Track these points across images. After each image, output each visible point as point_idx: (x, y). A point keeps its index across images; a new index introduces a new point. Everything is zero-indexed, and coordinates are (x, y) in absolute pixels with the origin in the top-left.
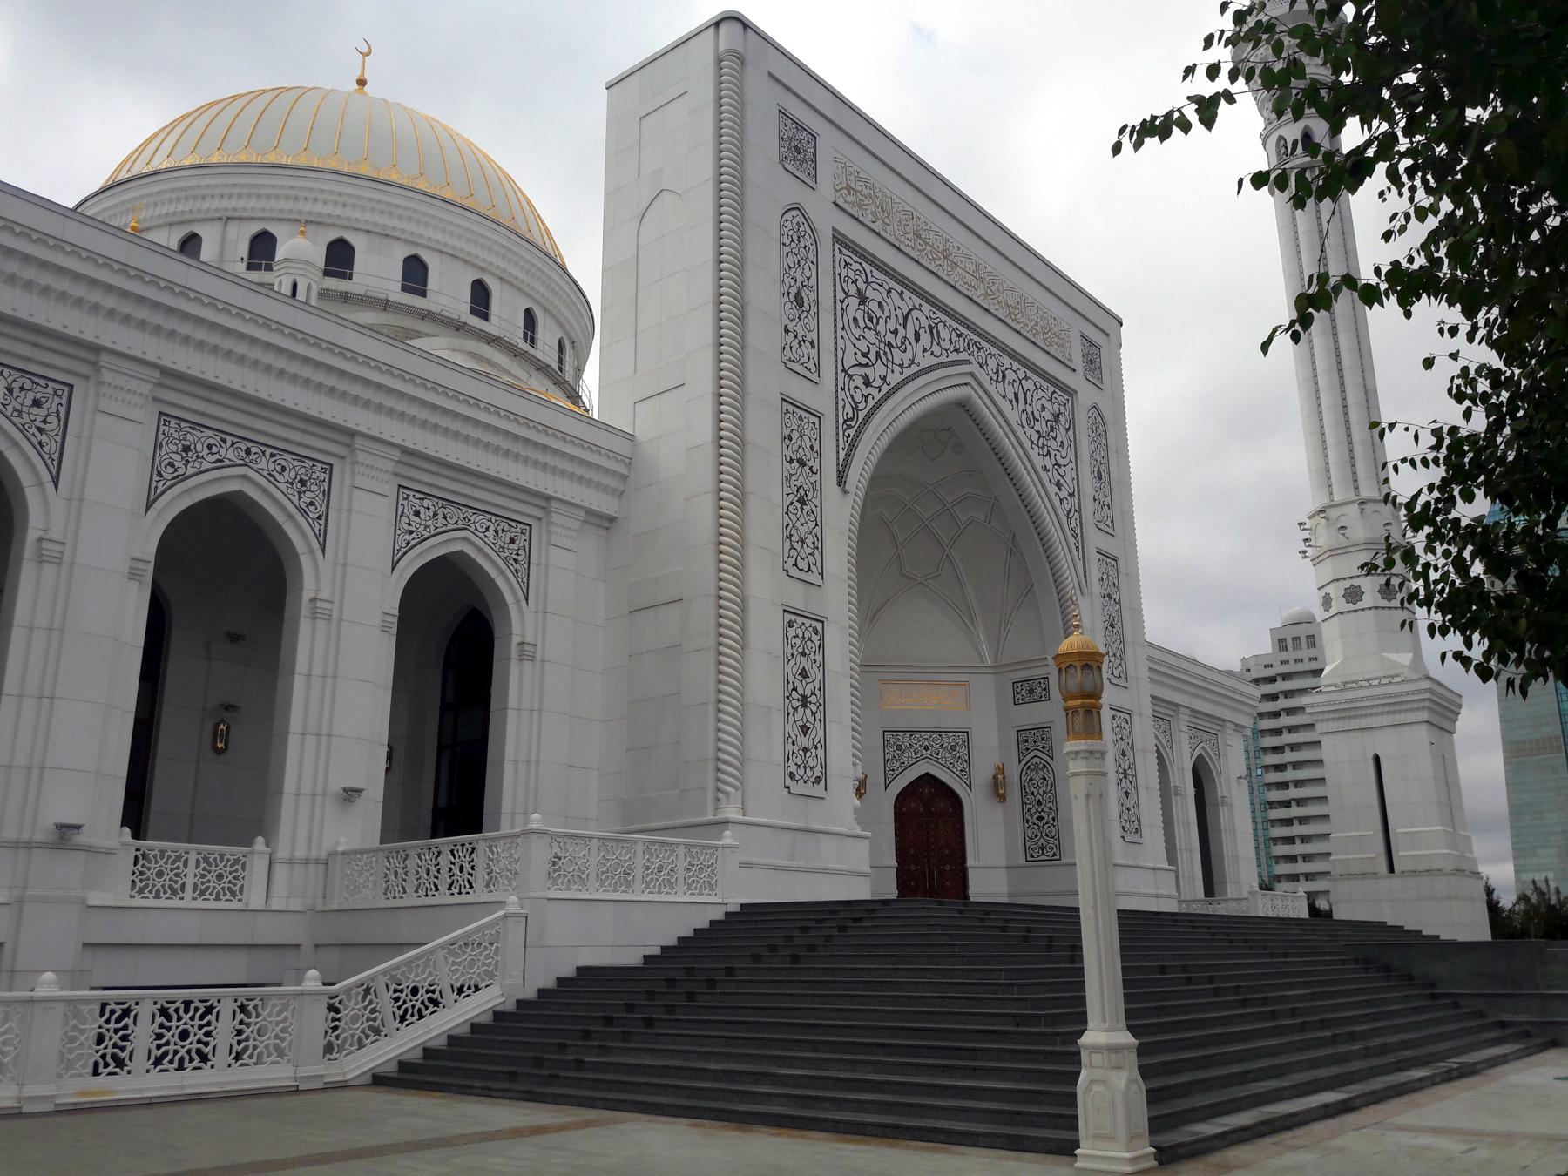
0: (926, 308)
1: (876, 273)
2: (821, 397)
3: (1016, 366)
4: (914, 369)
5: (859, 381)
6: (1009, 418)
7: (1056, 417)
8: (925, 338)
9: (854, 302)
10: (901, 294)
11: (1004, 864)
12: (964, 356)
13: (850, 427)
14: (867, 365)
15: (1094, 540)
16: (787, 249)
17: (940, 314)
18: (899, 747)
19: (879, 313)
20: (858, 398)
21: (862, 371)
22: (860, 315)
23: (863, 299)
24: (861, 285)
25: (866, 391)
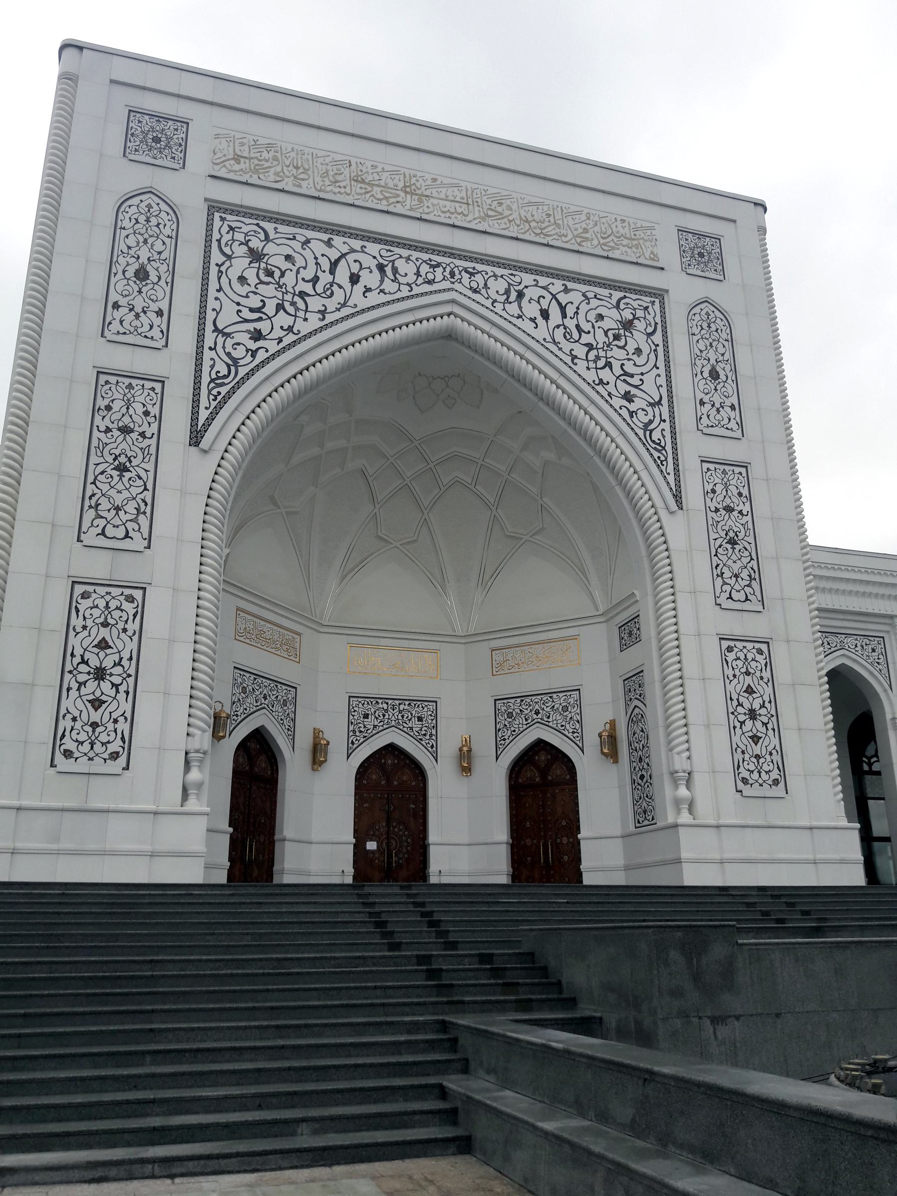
0: (373, 248)
1: (282, 228)
2: (175, 364)
3: (543, 281)
4: (345, 311)
5: (244, 338)
6: (520, 337)
7: (628, 325)
8: (370, 279)
9: (241, 264)
10: (329, 243)
11: (619, 833)
12: (446, 285)
13: (223, 384)
14: (260, 319)
15: (693, 447)
16: (125, 233)
17: (397, 250)
18: (510, 715)
19: (284, 265)
20: (239, 353)
21: (251, 326)
22: (251, 275)
23: (256, 256)
24: (255, 243)
25: (253, 346)
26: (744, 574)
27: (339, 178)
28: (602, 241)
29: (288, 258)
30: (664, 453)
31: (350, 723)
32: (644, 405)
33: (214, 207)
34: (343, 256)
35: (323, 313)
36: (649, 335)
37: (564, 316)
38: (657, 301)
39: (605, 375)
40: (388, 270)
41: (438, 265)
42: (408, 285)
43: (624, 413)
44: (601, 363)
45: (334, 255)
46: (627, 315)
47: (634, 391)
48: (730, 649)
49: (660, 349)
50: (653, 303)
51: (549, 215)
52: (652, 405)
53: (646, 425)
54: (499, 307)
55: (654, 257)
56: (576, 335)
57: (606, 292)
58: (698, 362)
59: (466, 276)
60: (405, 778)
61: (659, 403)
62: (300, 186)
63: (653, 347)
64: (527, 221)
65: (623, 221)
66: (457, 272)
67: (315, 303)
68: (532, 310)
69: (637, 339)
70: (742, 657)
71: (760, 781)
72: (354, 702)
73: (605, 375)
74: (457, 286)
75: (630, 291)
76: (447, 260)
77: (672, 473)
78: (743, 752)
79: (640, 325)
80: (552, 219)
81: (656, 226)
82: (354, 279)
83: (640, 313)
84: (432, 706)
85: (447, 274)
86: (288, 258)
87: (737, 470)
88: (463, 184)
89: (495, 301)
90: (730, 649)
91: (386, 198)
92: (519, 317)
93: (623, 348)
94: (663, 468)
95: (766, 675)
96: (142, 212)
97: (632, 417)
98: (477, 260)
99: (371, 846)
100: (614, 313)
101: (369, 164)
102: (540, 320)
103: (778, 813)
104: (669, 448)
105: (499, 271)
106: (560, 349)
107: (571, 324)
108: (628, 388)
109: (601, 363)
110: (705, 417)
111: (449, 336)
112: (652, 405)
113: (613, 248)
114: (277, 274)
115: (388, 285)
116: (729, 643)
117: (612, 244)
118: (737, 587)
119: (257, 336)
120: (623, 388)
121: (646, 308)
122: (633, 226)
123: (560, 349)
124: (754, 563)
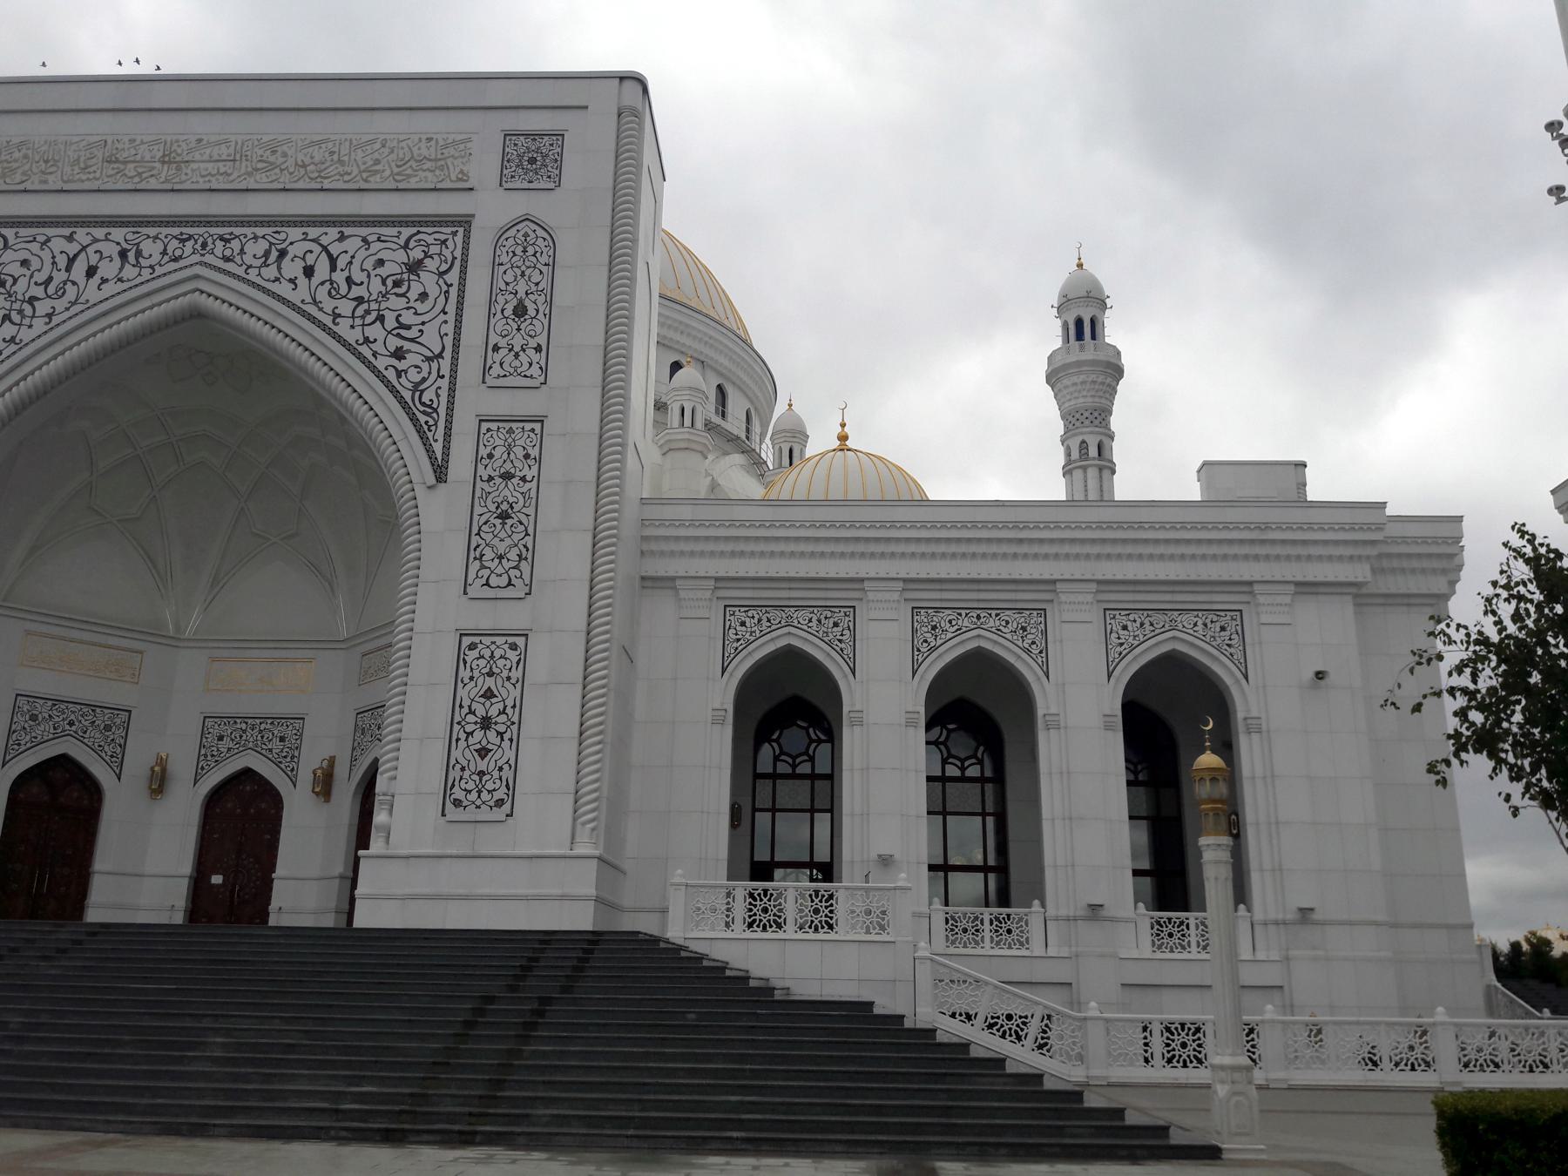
0: (118, 234)
1: (23, 232)
3: (313, 232)
6: (266, 307)
7: (414, 267)
8: (108, 269)
10: (70, 238)
12: (196, 258)
17: (144, 230)
26: (513, 555)
27: (90, 163)
28: (396, 170)
29: (25, 263)
30: (427, 418)
31: (201, 746)
32: (417, 360)
34: (84, 248)
35: (50, 316)
36: (441, 274)
37: (333, 268)
38: (461, 230)
39: (375, 332)
40: (131, 256)
41: (190, 237)
42: (151, 267)
43: (391, 375)
44: (369, 319)
45: (72, 249)
46: (417, 254)
47: (407, 345)
48: (472, 647)
49: (454, 292)
50: (455, 234)
51: (332, 153)
52: (429, 359)
53: (416, 385)
54: (253, 272)
55: (463, 176)
56: (344, 289)
57: (393, 231)
58: (501, 299)
59: (220, 244)
60: (263, 806)
61: (440, 355)
62: (46, 182)
63: (445, 288)
64: (304, 166)
65: (429, 140)
66: (210, 241)
67: (43, 307)
68: (292, 268)
69: (428, 280)
70: (487, 653)
71: (479, 802)
72: (209, 722)
73: (375, 332)
74: (209, 259)
75: (420, 224)
76: (201, 230)
77: (441, 440)
78: (463, 769)
79: (431, 264)
80: (335, 157)
81: (474, 137)
83: (434, 249)
84: (298, 724)
85: (198, 246)
86: (25, 263)
87: (528, 426)
88: (233, 138)
89: (250, 267)
90: (472, 647)
91: (140, 174)
92: (277, 279)
93: (403, 295)
94: (430, 435)
95: (515, 674)
97: (399, 375)
98: (230, 224)
99: (217, 879)
100: (401, 256)
101: (126, 139)
102: (302, 281)
103: (491, 840)
104: (442, 411)
105: (260, 231)
106: (321, 309)
107: (339, 277)
108: (400, 343)
109: (369, 319)
110: (496, 366)
111: (196, 315)
112: (429, 359)
113: (409, 176)
114: (10, 281)
116: (469, 640)
117: (409, 172)
118: (500, 570)
120: (393, 343)
121: (444, 242)
122: (441, 143)
123: (321, 309)
124: (529, 540)
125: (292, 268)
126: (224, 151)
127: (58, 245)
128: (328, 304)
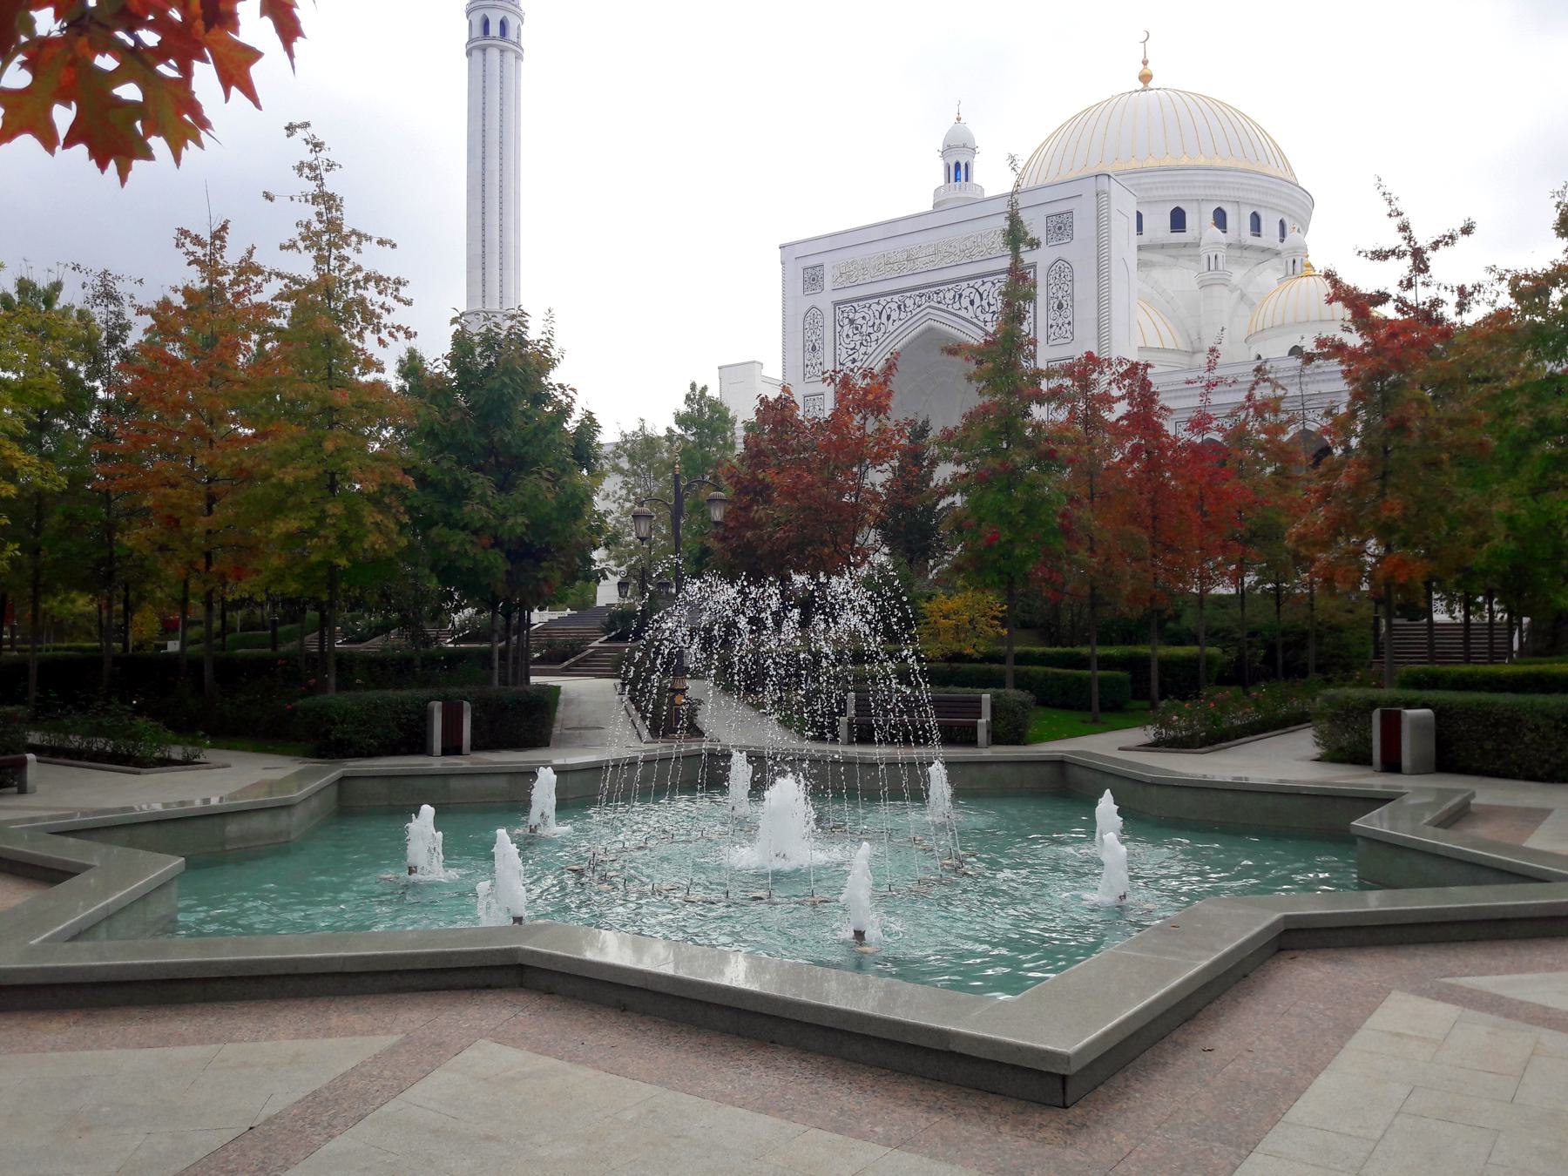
0: (896, 298)
3: (971, 283)
8: (894, 316)
9: (847, 329)
23: (852, 322)
33: (836, 304)
67: (874, 337)
68: (965, 302)
82: (889, 317)
96: (811, 318)
111: (930, 330)
115: (903, 315)
119: (854, 361)
125: (965, 302)
126: (931, 250)
127: (874, 307)
128: (982, 317)
